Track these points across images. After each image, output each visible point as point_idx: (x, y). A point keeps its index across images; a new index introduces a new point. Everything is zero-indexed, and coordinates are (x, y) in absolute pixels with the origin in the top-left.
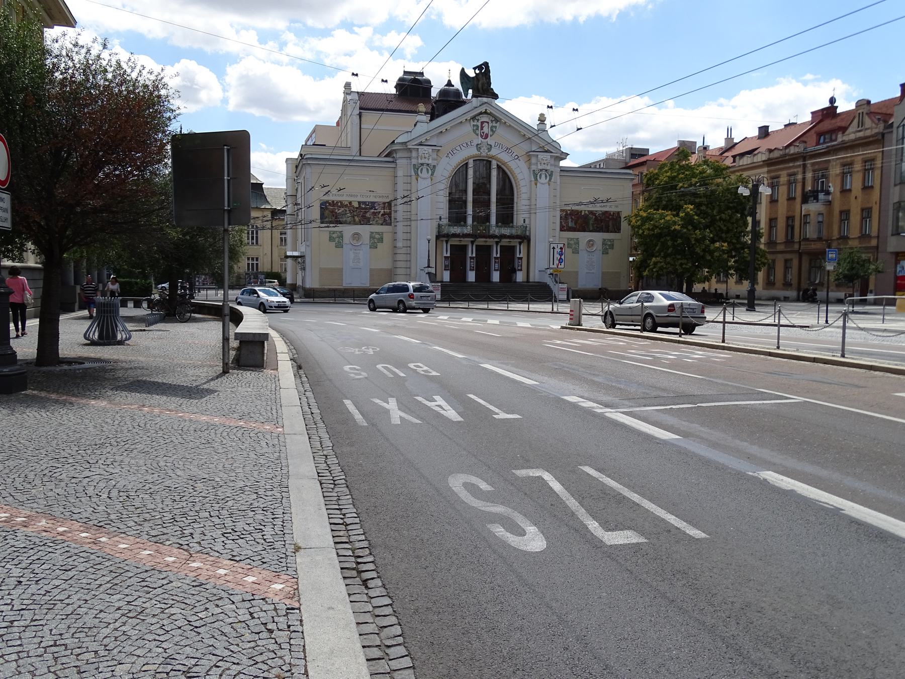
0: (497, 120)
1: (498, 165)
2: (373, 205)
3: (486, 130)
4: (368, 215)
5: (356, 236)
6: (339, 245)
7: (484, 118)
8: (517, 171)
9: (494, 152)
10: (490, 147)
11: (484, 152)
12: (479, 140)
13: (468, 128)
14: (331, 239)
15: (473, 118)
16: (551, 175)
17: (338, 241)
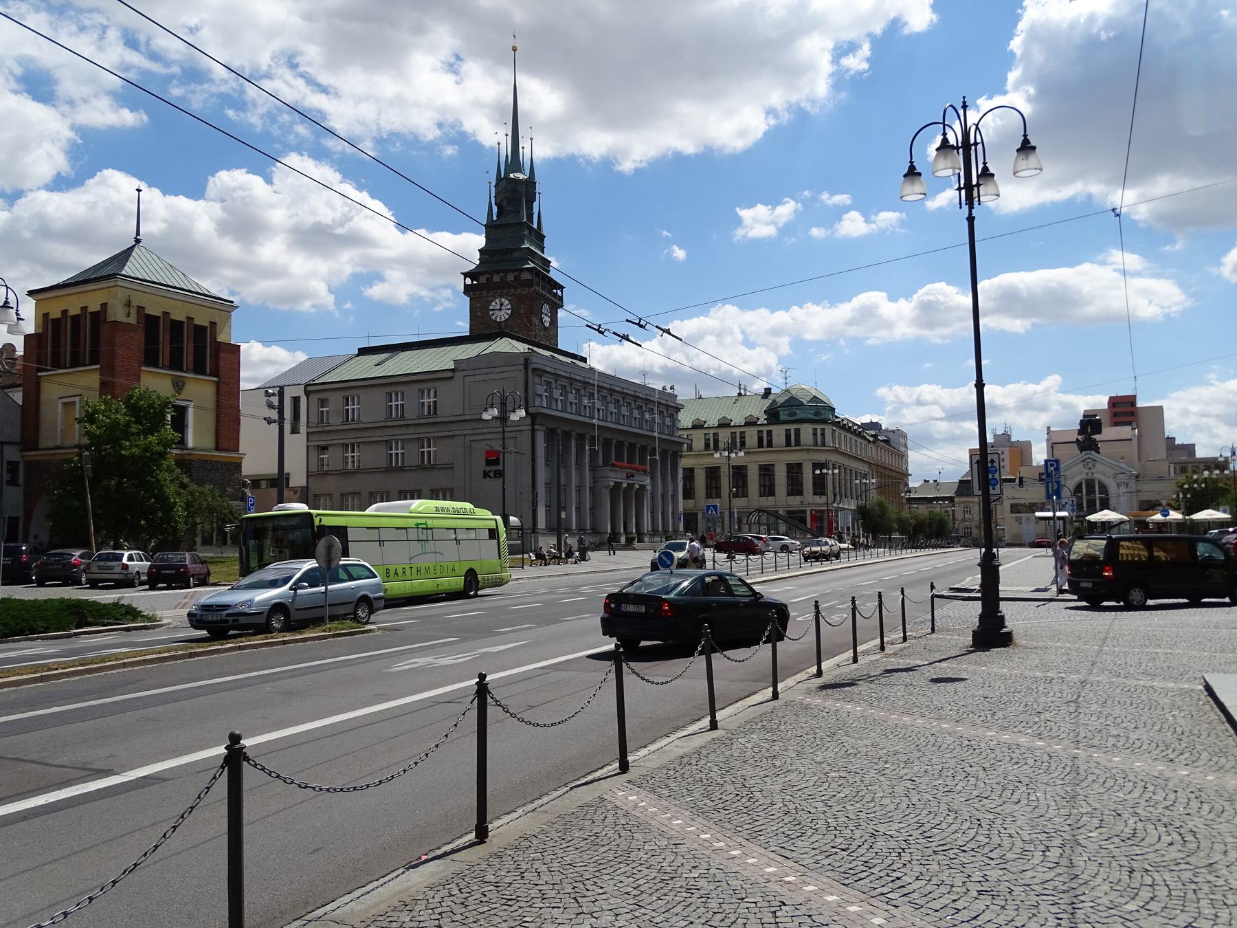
0: (1095, 461)
1: (1099, 482)
2: (1036, 504)
3: (1090, 465)
4: (1034, 508)
5: (1028, 519)
6: (1021, 523)
7: (1089, 460)
8: (1108, 484)
9: (1096, 476)
10: (1093, 473)
11: (1090, 476)
12: (1087, 471)
13: (1081, 465)
14: (1016, 521)
15: (1083, 461)
16: (1127, 484)
17: (1019, 521)
